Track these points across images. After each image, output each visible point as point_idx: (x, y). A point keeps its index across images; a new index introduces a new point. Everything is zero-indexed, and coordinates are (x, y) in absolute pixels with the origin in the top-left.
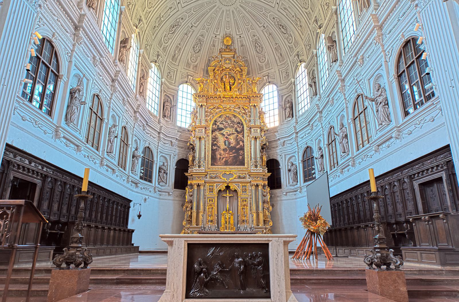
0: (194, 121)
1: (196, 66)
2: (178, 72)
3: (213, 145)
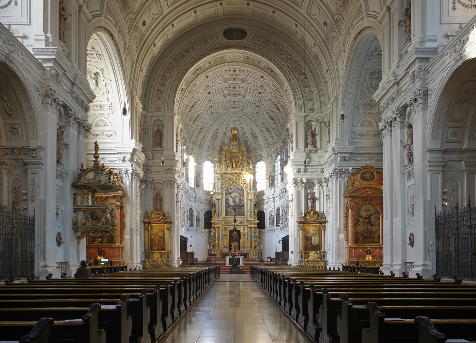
0: (214, 188)
1: (214, 148)
2: (203, 155)
3: (226, 203)
